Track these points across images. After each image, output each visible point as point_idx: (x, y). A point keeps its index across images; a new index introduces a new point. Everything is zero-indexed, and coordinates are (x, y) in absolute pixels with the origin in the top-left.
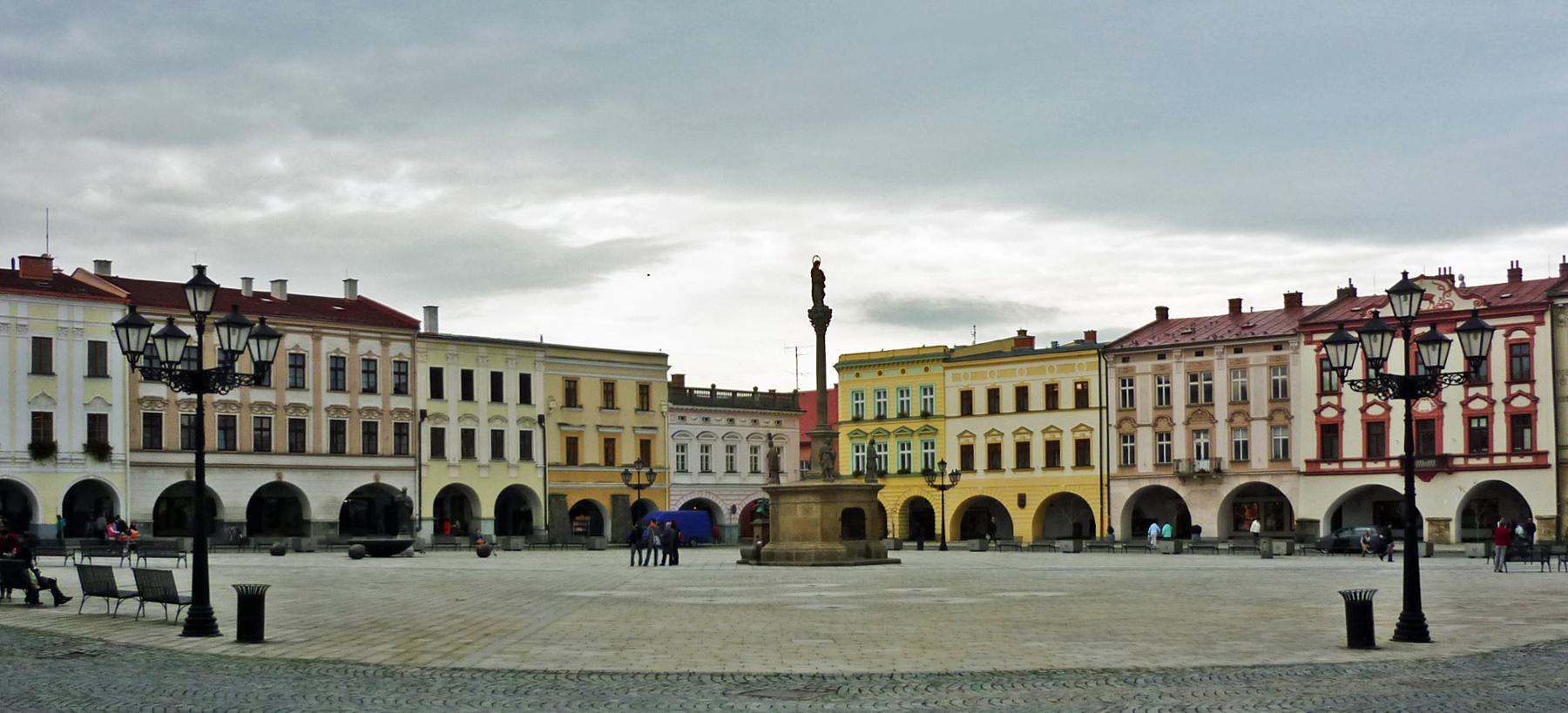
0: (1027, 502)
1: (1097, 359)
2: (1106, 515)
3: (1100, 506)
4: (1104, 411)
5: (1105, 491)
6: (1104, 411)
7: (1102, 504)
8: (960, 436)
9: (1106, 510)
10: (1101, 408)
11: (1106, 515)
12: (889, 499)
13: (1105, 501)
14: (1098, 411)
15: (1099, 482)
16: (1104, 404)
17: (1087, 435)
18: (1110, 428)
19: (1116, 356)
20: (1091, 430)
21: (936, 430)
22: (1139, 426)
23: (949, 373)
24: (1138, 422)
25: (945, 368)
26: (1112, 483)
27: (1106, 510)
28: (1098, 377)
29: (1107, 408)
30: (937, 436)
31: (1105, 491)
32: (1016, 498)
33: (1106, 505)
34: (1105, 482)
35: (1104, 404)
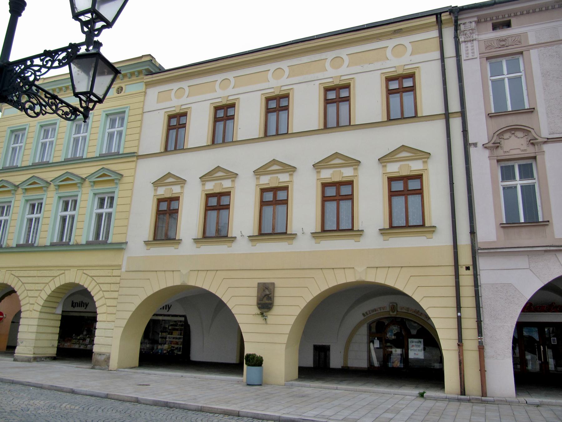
0: (277, 301)
1: (434, 33)
2: (470, 333)
3: (453, 312)
4: (456, 124)
5: (466, 279)
6: (456, 124)
7: (459, 308)
8: (157, 184)
9: (469, 323)
10: (447, 116)
11: (470, 333)
12: (28, 287)
13: (468, 301)
14: (441, 124)
15: (451, 262)
16: (454, 106)
17: (416, 166)
18: (472, 150)
19: (478, 22)
20: (425, 156)
21: (122, 175)
22: (548, 141)
23: (153, 92)
24: (545, 133)
25: (148, 85)
26: (482, 263)
27: (469, 323)
28: (438, 64)
29: (463, 114)
30: (121, 187)
31: (466, 279)
32: (254, 292)
33: (469, 313)
34: (465, 259)
35: (454, 106)
